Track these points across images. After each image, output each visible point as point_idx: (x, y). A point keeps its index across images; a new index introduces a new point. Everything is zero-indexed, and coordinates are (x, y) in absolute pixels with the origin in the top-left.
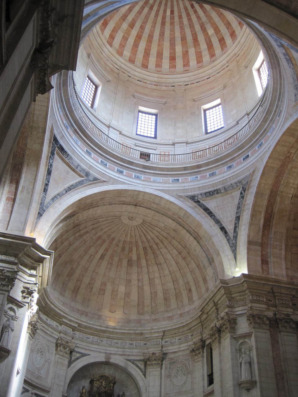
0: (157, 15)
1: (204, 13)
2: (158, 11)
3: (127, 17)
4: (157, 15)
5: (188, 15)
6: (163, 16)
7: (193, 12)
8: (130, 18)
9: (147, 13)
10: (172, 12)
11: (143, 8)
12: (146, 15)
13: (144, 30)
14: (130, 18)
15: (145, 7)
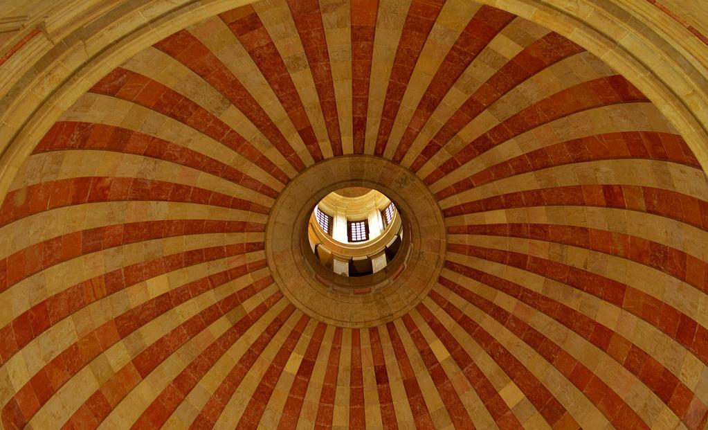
0: (250, 358)
1: (416, 413)
2: (261, 345)
3: (140, 326)
4: (250, 358)
5: (357, 398)
6: (271, 367)
7: (376, 396)
8: (151, 333)
9: (220, 338)
10: (307, 368)
11: (211, 315)
12: (215, 344)
13: (186, 394)
14: (151, 333)
15: (220, 315)
